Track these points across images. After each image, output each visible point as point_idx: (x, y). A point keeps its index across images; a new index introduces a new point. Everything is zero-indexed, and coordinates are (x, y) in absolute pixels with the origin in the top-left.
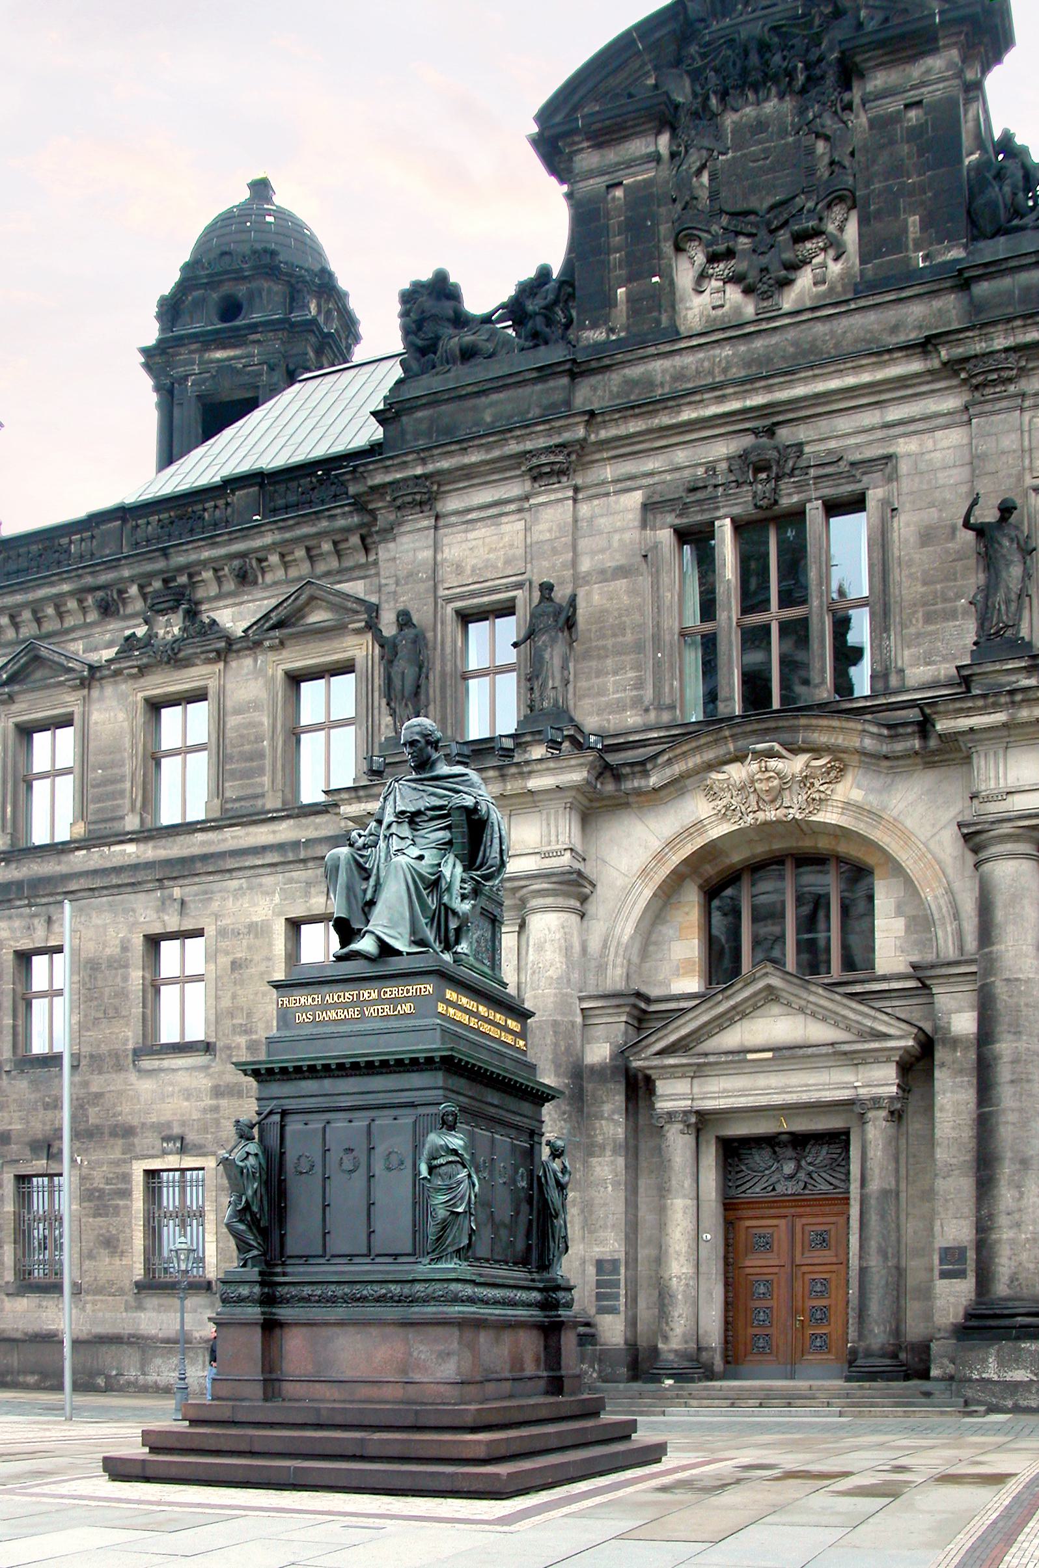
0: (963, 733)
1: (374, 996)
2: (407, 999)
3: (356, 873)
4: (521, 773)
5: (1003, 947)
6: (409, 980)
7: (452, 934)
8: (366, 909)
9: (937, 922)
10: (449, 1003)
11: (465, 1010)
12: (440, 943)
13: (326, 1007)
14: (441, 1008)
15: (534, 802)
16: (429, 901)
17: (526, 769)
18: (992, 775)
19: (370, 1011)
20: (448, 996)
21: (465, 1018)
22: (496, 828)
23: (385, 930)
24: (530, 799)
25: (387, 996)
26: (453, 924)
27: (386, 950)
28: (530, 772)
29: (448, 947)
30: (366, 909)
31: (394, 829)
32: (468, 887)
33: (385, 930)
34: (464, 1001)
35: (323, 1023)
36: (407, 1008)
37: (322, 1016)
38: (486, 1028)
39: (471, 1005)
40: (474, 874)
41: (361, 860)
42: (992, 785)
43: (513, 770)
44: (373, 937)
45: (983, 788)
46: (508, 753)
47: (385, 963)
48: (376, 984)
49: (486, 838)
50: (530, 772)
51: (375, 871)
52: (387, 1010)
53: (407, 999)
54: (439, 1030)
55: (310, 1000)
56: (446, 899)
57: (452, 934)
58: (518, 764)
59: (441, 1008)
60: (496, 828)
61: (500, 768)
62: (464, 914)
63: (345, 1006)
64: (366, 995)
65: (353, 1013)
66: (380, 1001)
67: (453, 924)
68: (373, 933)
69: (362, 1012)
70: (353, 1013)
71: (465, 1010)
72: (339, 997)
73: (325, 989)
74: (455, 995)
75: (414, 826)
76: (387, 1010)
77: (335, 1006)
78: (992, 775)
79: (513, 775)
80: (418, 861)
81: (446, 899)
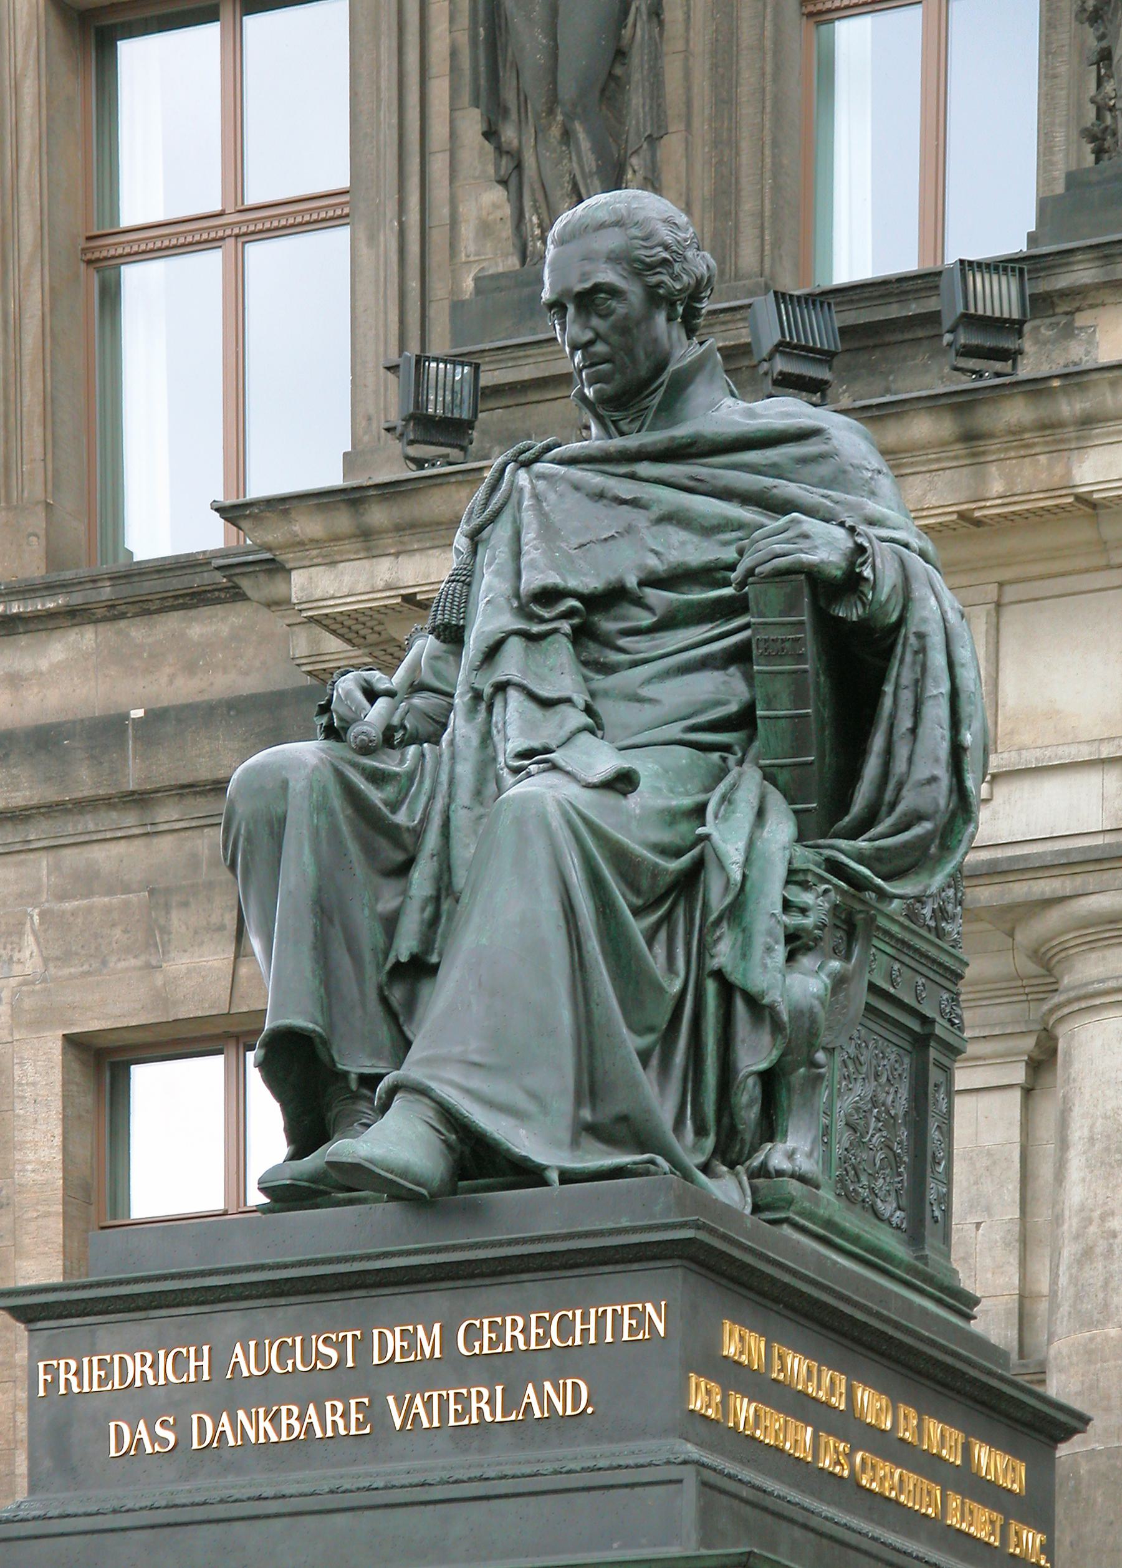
1: (429, 1342)
2: (560, 1362)
3: (353, 847)
4: (1046, 426)
6: (570, 1283)
7: (747, 1097)
8: (397, 995)
10: (735, 1377)
11: (801, 1406)
12: (701, 1131)
14: (702, 1397)
15: (1103, 546)
16: (656, 960)
17: (1069, 408)
20: (730, 1349)
21: (799, 1439)
22: (938, 659)
23: (476, 1082)
24: (1082, 533)
26: (755, 1054)
27: (478, 1160)
28: (1087, 422)
29: (729, 1151)
30: (397, 995)
31: (512, 663)
32: (817, 903)
33: (476, 1082)
34: (796, 1366)
36: (564, 1397)
38: (884, 1478)
39: (826, 1384)
40: (844, 849)
41: (376, 796)
43: (1017, 411)
44: (428, 1112)
46: (993, 340)
47: (474, 1212)
48: (439, 1299)
49: (894, 698)
50: (1087, 422)
51: (432, 840)
52: (485, 1404)
53: (560, 1362)
54: (691, 1486)
55: (166, 1366)
56: (723, 954)
57: (747, 1097)
58: (1036, 388)
59: (702, 1397)
60: (938, 659)
61: (960, 404)
62: (797, 1014)
63: (312, 1388)
64: (395, 1342)
65: (338, 1418)
66: (453, 1368)
67: (755, 1054)
68: (421, 1091)
69: (375, 1414)
70: (338, 1418)
71: (801, 1406)
73: (229, 1320)
74: (757, 1344)
75: (594, 651)
76: (485, 1404)
77: (267, 1391)
79: (1017, 431)
80: (610, 798)
81: (723, 954)
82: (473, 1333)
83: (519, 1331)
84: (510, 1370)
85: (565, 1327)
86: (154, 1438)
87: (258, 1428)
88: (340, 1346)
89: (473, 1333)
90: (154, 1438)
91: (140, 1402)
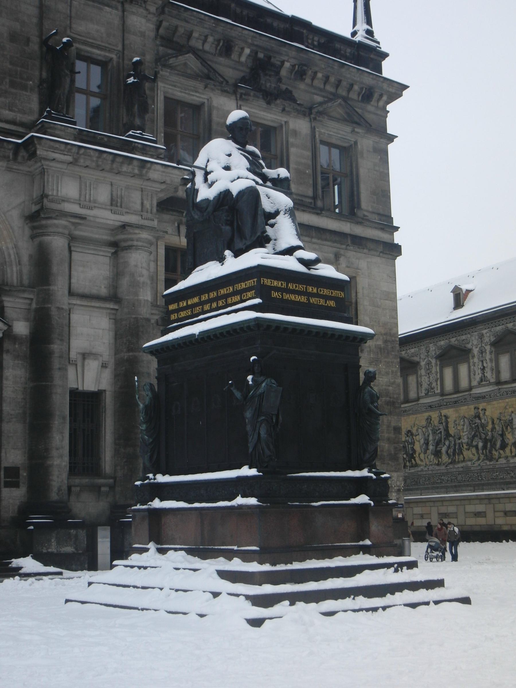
0: (46, 159)
1: (315, 291)
5: (55, 288)
9: (8, 263)
13: (288, 291)
18: (55, 187)
19: (313, 300)
25: (322, 293)
35: (287, 301)
36: (332, 303)
37: (286, 296)
42: (55, 194)
45: (50, 193)
52: (322, 302)
55: (280, 284)
63: (300, 293)
64: (311, 289)
65: (303, 299)
66: (317, 295)
72: (296, 287)
76: (322, 302)
77: (293, 292)
78: (55, 187)
82: (320, 291)
83: (326, 292)
84: (327, 298)
85: (332, 293)
86: (279, 295)
87: (292, 297)
88: (303, 287)
89: (320, 291)
90: (279, 295)
91: (277, 289)
